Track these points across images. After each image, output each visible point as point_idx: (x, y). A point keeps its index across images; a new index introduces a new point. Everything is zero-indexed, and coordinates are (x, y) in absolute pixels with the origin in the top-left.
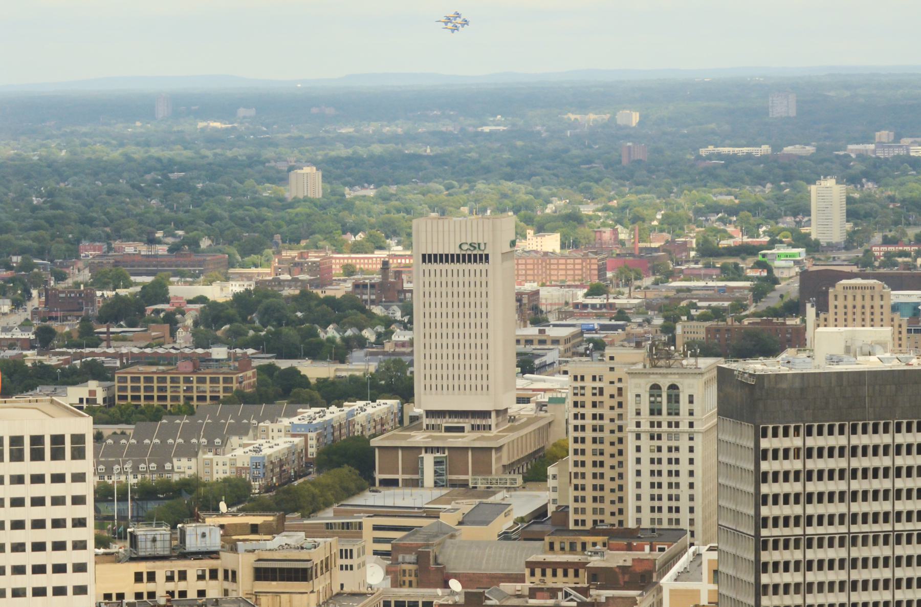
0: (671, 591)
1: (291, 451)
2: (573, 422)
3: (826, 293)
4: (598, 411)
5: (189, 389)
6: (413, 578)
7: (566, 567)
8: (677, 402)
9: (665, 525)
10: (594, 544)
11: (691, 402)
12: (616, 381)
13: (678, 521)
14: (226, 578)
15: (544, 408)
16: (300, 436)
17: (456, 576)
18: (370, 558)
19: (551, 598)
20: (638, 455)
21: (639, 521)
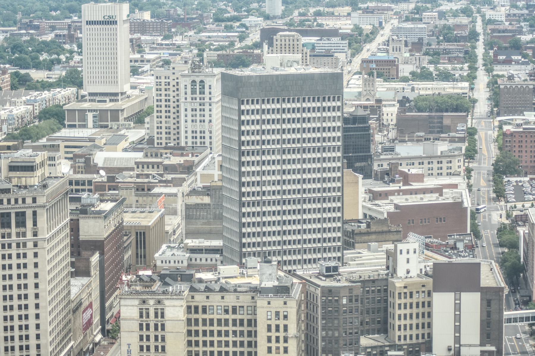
2: (156, 98)
3: (273, 38)
4: (167, 93)
6: (83, 170)
7: (153, 164)
8: (204, 88)
10: (166, 154)
11: (210, 88)
13: (204, 143)
18: (63, 161)
19: (147, 178)
21: (186, 143)
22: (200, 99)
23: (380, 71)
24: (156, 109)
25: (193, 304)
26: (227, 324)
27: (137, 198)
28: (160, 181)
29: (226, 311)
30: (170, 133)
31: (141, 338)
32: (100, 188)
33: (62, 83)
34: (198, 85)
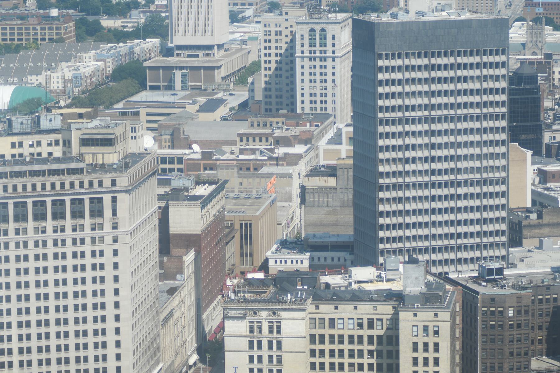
0: (324, 150)
1: (97, 70)
2: (264, 51)
4: (278, 45)
5: (36, 34)
8: (325, 38)
9: (318, 111)
10: (277, 123)
12: (289, 27)
13: (326, 109)
14: (64, 144)
15: (245, 43)
16: (101, 61)
17: (196, 142)
18: (144, 131)
19: (252, 154)
20: (302, 70)
21: (303, 109)
22: (321, 53)
23: (549, 16)
24: (263, 65)
25: (317, 316)
26: (361, 342)
27: (240, 180)
28: (271, 158)
29: (361, 326)
30: (281, 97)
31: (251, 358)
32: (193, 165)
33: (142, 32)
34: (318, 36)
